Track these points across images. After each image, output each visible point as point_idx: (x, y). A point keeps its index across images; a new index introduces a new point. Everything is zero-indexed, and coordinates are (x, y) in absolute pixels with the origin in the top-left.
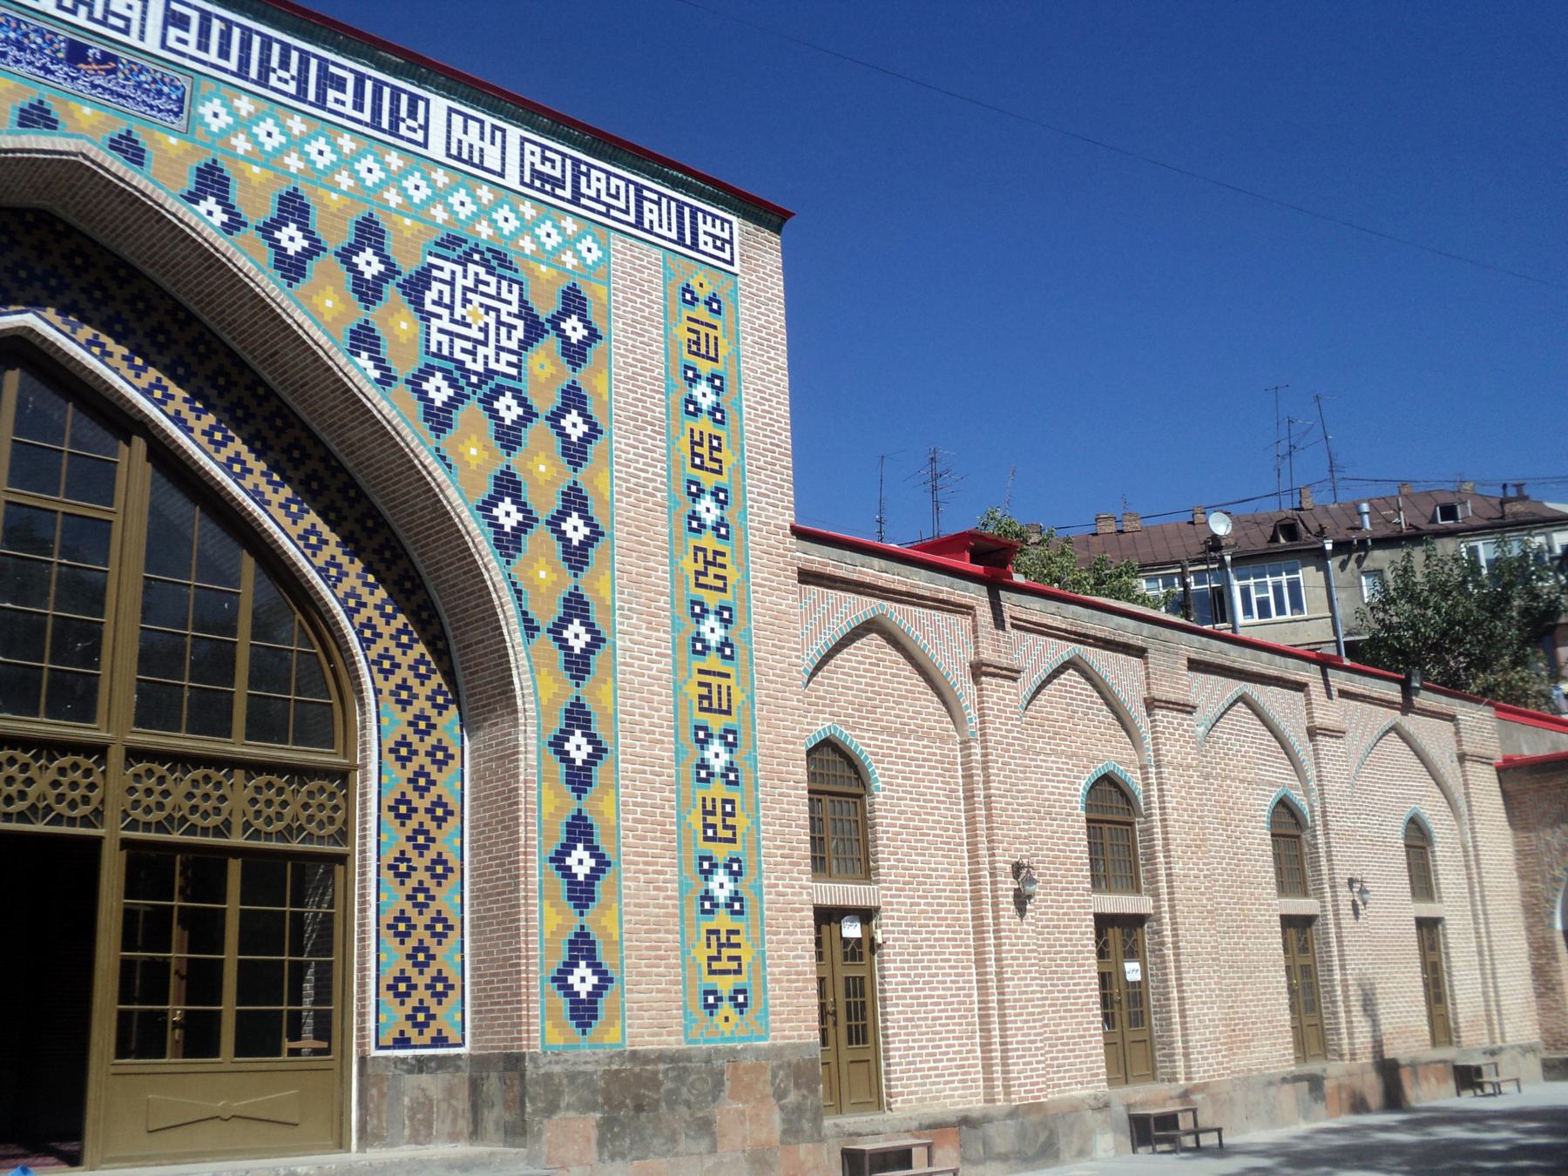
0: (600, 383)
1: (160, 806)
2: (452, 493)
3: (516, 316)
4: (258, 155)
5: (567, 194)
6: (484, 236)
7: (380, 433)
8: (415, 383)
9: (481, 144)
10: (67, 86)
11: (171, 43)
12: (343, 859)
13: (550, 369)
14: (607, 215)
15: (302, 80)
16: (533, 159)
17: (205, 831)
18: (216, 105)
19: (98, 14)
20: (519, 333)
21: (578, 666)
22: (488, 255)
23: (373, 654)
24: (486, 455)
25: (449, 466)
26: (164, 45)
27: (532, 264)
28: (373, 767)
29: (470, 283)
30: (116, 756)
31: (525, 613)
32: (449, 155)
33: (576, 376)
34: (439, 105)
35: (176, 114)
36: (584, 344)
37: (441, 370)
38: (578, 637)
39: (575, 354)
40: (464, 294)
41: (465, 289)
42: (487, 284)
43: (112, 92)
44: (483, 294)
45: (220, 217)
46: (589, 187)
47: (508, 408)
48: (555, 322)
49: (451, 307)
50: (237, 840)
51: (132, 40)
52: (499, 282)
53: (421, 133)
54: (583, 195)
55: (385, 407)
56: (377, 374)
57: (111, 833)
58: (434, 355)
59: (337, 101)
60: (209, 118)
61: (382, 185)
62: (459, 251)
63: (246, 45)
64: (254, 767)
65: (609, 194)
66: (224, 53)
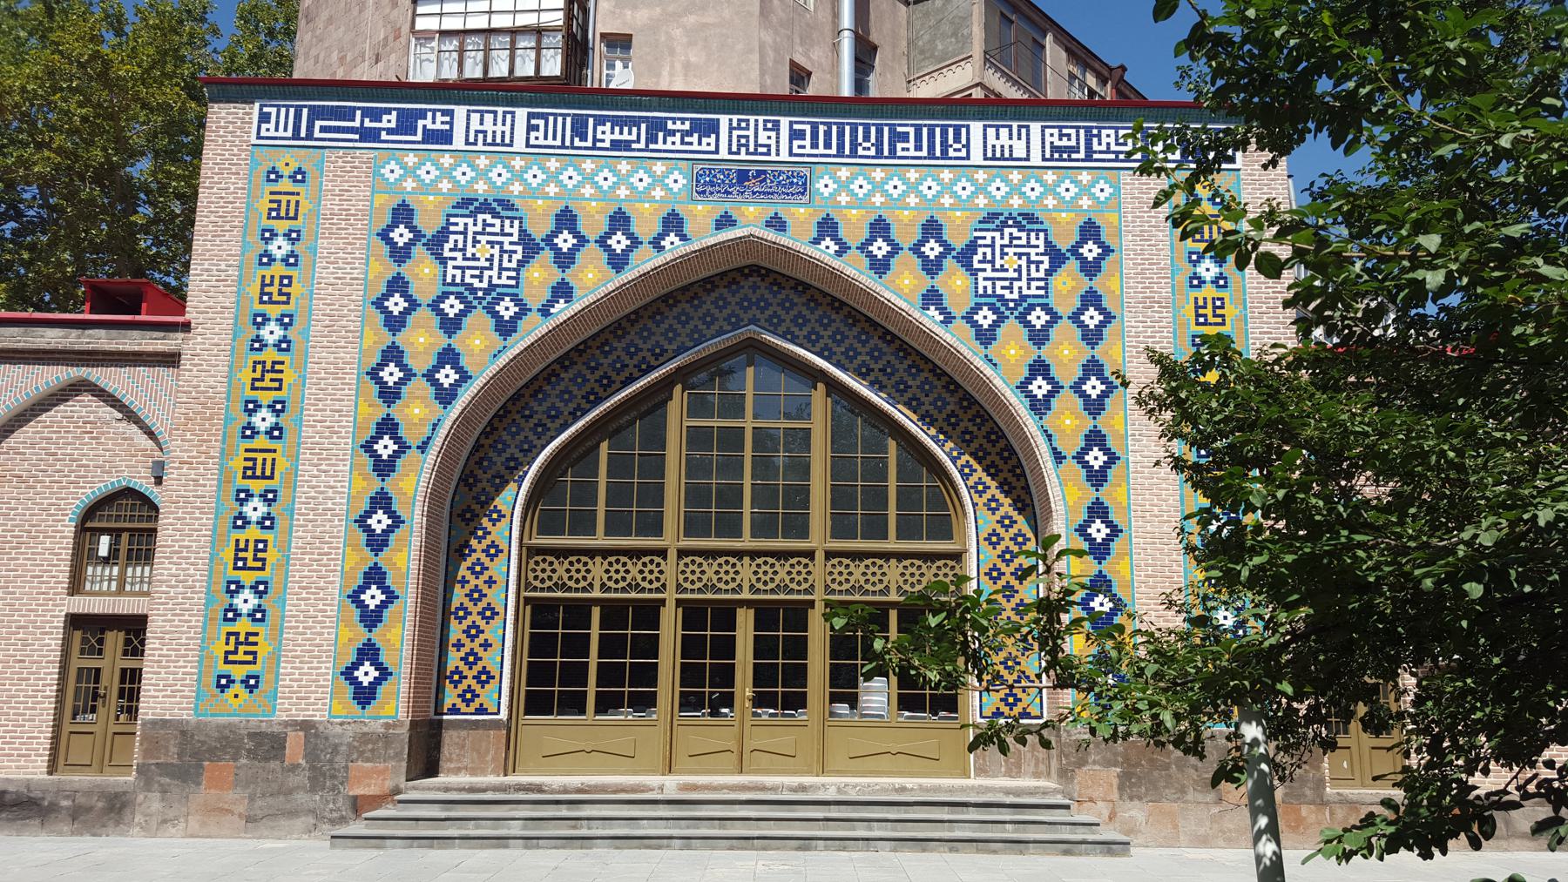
0: (1114, 284)
1: (847, 581)
2: (998, 382)
3: (1042, 254)
4: (856, 203)
5: (1082, 155)
6: (1016, 206)
7: (950, 353)
8: (969, 318)
9: (1011, 142)
10: (740, 198)
11: (796, 150)
13: (1071, 283)
14: (1117, 160)
15: (879, 145)
16: (1052, 139)
17: (874, 593)
18: (826, 180)
19: (752, 150)
20: (1046, 265)
21: (1097, 478)
22: (1019, 219)
23: (971, 483)
24: (1022, 352)
25: (995, 365)
26: (791, 154)
27: (1054, 215)
28: (973, 550)
29: (1006, 241)
30: (820, 556)
31: (1054, 449)
32: (986, 159)
33: (1092, 284)
34: (976, 127)
35: (803, 194)
36: (1098, 260)
37: (986, 304)
38: (1096, 458)
39: (1091, 269)
40: (1002, 250)
41: (1002, 246)
42: (1020, 238)
43: (764, 193)
44: (1016, 246)
45: (834, 247)
46: (1100, 144)
47: (1038, 318)
48: (1074, 251)
49: (992, 262)
50: (894, 597)
51: (773, 157)
52: (1028, 235)
53: (964, 150)
54: (1095, 152)
55: (948, 337)
56: (941, 318)
57: (818, 596)
58: (981, 296)
59: (903, 149)
60: (823, 189)
61: (940, 194)
62: (997, 222)
63: (841, 135)
64: (900, 556)
65: (1117, 144)
66: (828, 145)
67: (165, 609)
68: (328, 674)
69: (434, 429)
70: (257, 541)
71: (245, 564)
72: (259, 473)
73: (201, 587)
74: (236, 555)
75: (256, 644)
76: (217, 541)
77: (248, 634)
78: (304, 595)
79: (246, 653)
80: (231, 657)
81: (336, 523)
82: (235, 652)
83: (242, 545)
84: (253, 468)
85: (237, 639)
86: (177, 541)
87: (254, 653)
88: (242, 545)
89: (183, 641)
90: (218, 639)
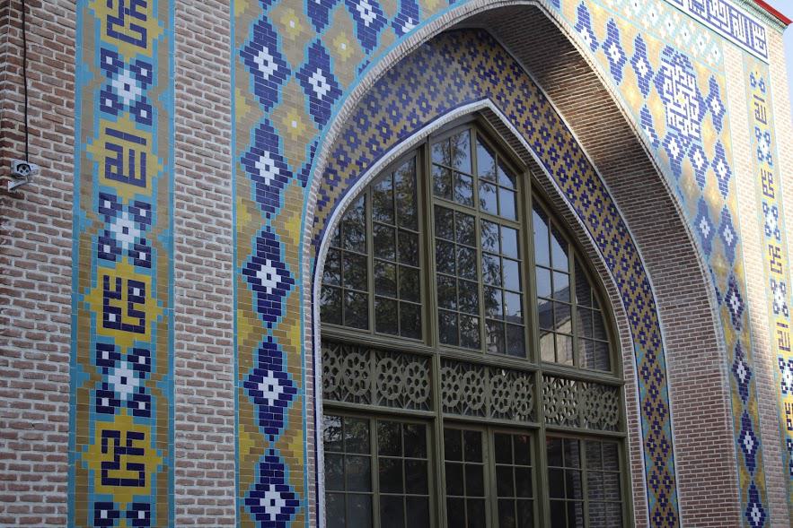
12: (622, 439)
67: (15, 385)
68: (230, 502)
69: (312, 155)
70: (132, 284)
71: (118, 318)
72: (126, 173)
73: (64, 350)
74: (106, 302)
75: (140, 452)
76: (81, 279)
77: (132, 435)
78: (195, 378)
79: (131, 467)
80: (112, 474)
81: (223, 270)
82: (116, 465)
83: (113, 288)
84: (119, 162)
85: (117, 443)
86: (25, 265)
87: (140, 467)
88: (113, 288)
89: (45, 443)
90: (93, 441)
